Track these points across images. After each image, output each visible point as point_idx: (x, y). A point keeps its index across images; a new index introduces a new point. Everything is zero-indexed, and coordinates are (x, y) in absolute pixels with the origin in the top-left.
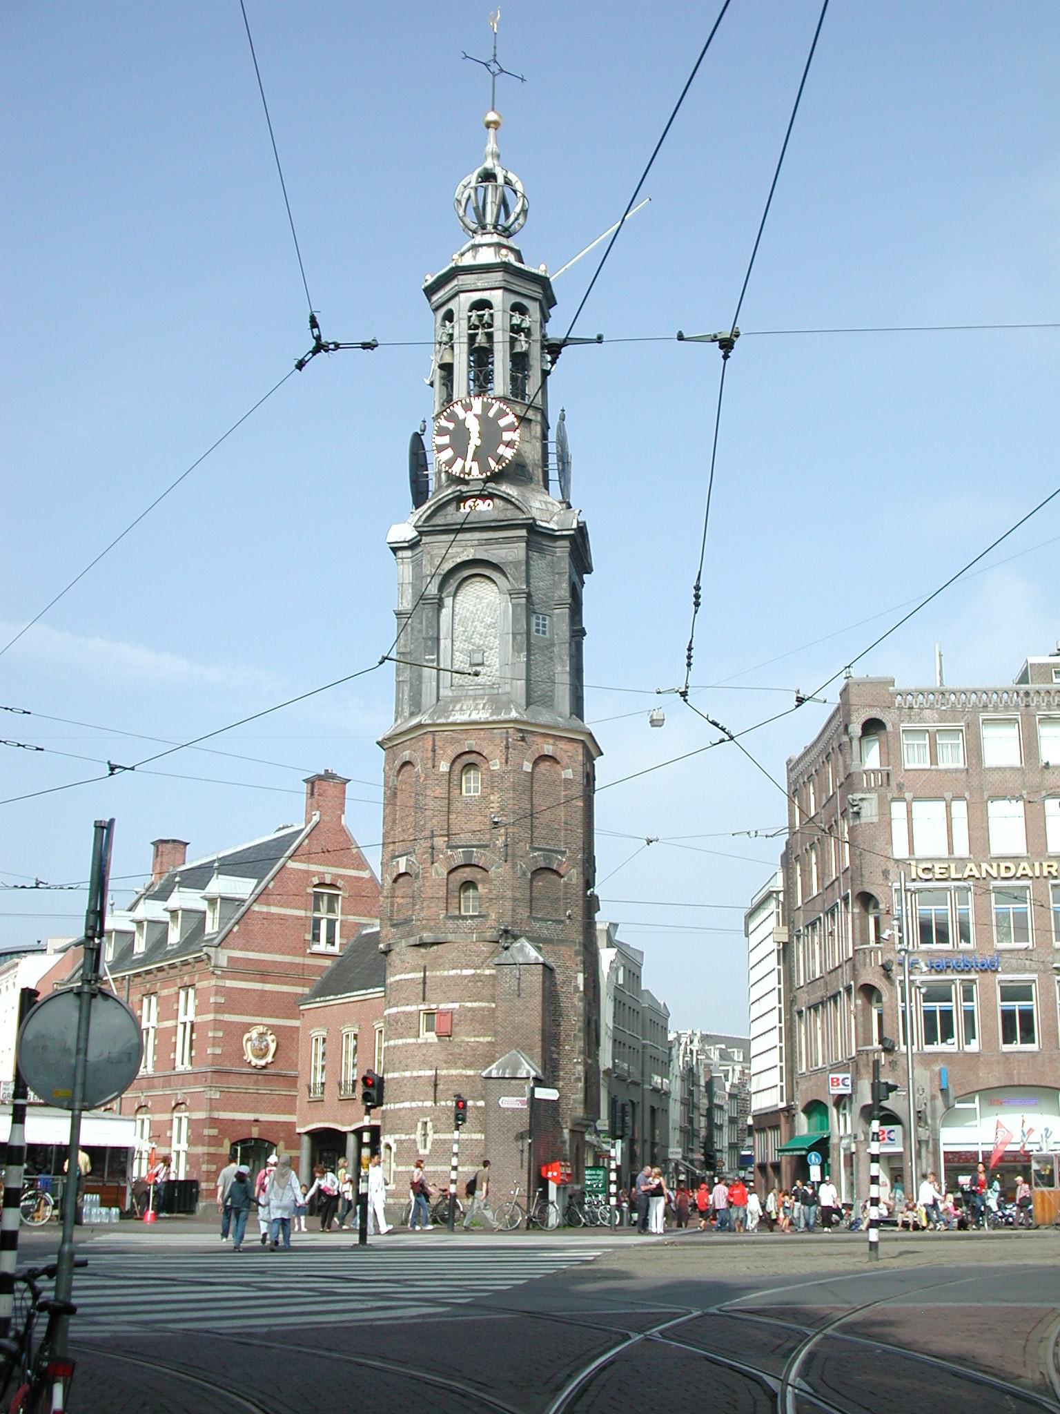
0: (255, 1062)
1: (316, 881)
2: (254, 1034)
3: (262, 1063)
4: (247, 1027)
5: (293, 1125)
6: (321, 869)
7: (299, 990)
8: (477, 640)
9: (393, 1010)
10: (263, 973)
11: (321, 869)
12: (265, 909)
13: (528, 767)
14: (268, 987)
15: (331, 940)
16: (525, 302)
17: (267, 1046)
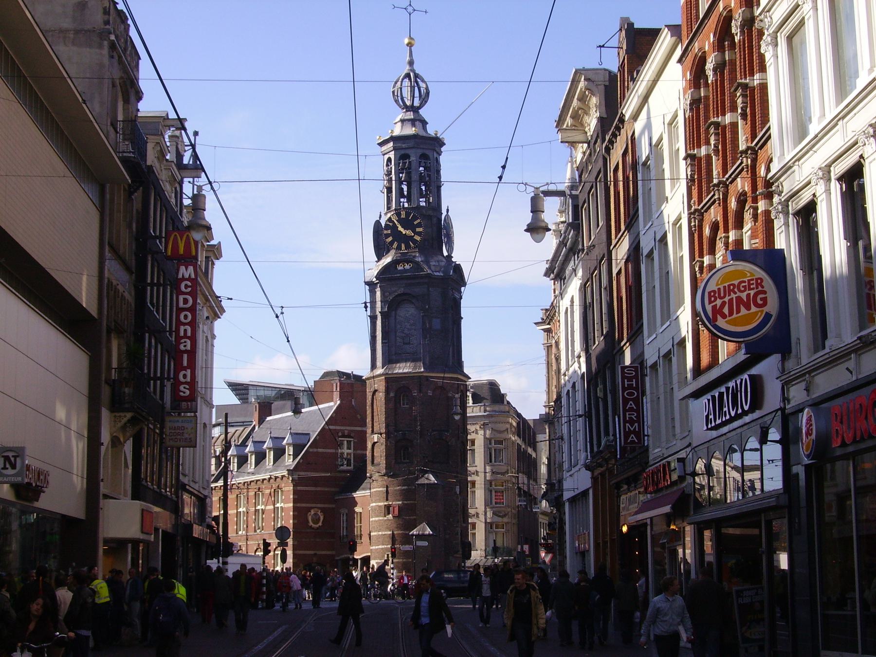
0: (314, 525)
1: (340, 434)
2: (312, 512)
3: (317, 526)
4: (309, 509)
5: (333, 556)
6: (342, 428)
7: (333, 489)
8: (406, 331)
9: (374, 504)
10: (315, 482)
11: (342, 428)
12: (315, 450)
13: (430, 393)
14: (319, 489)
15: (349, 464)
16: (427, 152)
17: (319, 519)
